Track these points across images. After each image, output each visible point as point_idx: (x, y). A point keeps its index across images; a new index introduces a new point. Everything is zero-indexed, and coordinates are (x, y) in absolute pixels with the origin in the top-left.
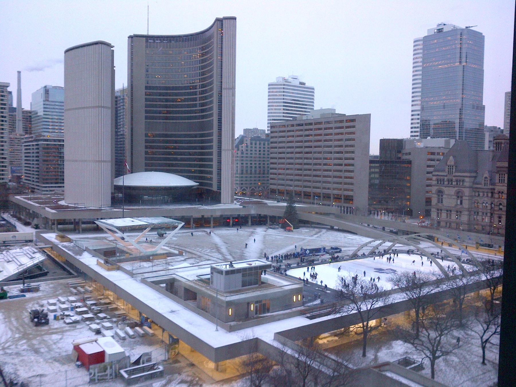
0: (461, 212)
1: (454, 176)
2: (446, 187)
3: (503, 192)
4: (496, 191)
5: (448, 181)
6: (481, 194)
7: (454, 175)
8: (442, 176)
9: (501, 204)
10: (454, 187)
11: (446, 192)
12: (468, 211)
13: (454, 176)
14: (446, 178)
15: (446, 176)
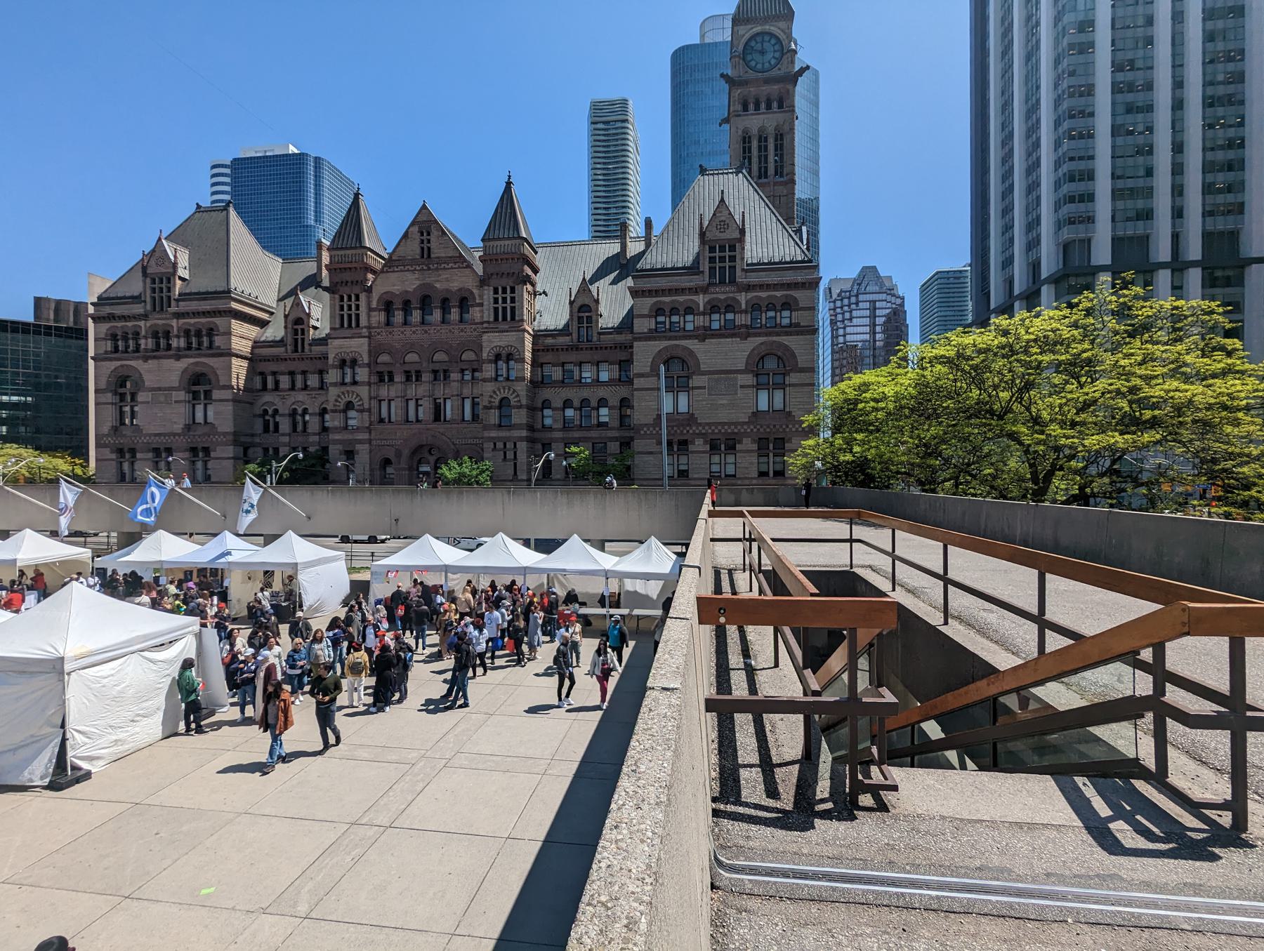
0: (207, 451)
1: (178, 315)
2: (146, 359)
3: (354, 363)
4: (330, 361)
5: (155, 335)
6: (285, 381)
7: (173, 309)
8: (124, 318)
9: (349, 406)
10: (178, 358)
11: (149, 380)
12: (236, 443)
13: (178, 315)
14: (142, 323)
15: (145, 317)
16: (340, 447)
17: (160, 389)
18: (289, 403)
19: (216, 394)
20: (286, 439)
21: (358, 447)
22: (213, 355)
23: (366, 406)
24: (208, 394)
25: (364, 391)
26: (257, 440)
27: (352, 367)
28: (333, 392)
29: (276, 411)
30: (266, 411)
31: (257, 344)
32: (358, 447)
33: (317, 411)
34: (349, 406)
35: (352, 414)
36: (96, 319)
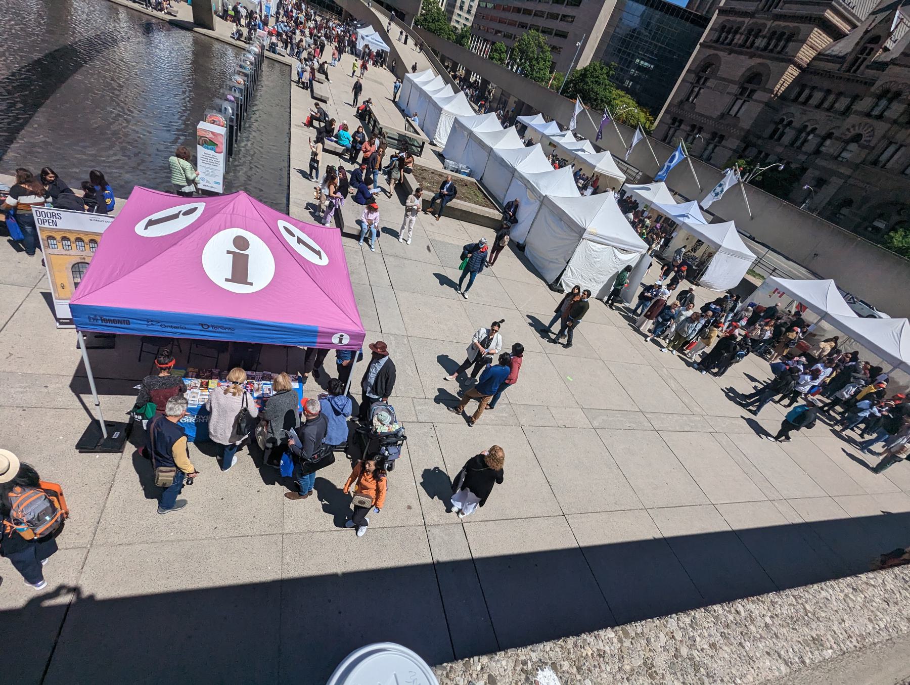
0: (722, 138)
10: (752, 56)
16: (817, 173)
17: (724, 79)
18: (805, 118)
19: (757, 95)
20: (779, 150)
21: (834, 179)
22: (777, 59)
23: (872, 144)
24: (753, 91)
25: (881, 128)
26: (760, 142)
27: (890, 101)
28: (852, 119)
29: (790, 123)
30: (783, 120)
31: (820, 56)
32: (834, 179)
33: (824, 133)
34: (857, 138)
35: (853, 147)
36: (722, 12)
